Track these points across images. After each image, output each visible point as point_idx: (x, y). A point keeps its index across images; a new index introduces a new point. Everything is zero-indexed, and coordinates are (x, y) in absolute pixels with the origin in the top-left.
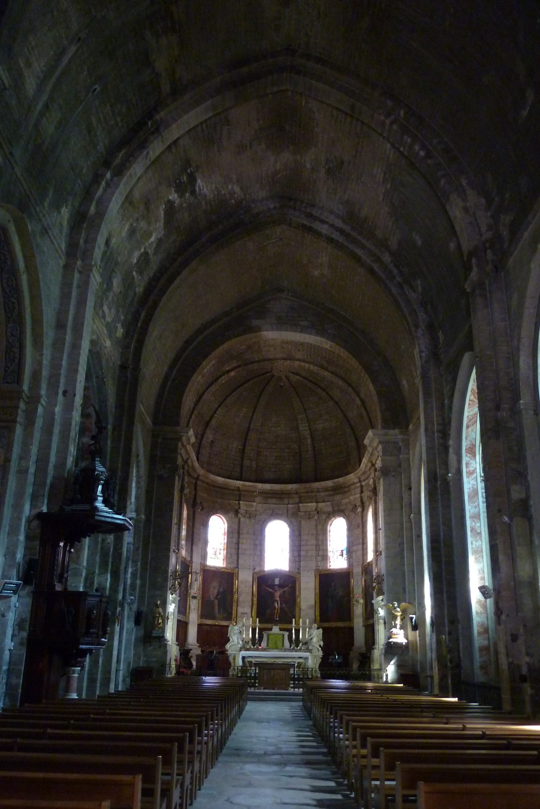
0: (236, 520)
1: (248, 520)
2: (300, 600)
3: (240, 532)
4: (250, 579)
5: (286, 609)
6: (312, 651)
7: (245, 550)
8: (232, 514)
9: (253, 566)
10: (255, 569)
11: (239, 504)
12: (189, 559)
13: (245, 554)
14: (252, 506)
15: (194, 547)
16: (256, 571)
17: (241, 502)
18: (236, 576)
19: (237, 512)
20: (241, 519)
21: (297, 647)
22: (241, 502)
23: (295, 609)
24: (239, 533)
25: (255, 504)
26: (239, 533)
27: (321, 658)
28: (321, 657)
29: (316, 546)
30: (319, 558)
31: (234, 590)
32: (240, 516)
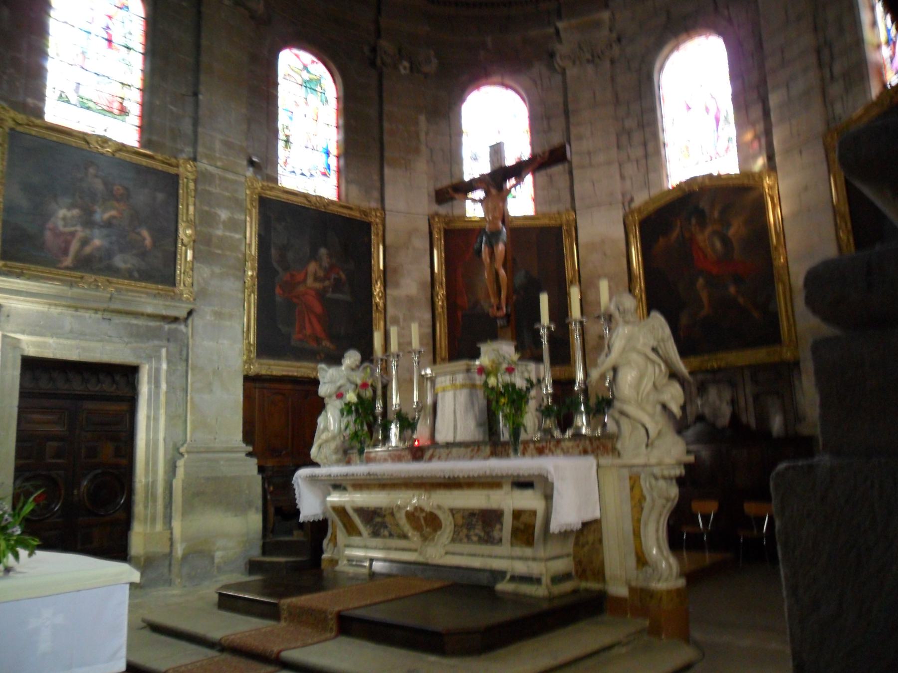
0: (558, 78)
1: (590, 68)
2: (786, 259)
3: (571, 107)
4: (619, 232)
5: (741, 300)
6: (619, 446)
7: (589, 153)
8: (539, 68)
9: (623, 195)
10: (632, 200)
11: (557, 32)
12: (374, 205)
13: (591, 165)
14: (597, 24)
15: (387, 171)
16: (637, 203)
17: (560, 25)
18: (570, 235)
19: (552, 55)
20: (568, 72)
21: (563, 431)
22: (560, 25)
23: (771, 296)
24: (567, 113)
25: (605, 15)
26: (567, 113)
27: (680, 481)
28: (679, 471)
29: (818, 52)
30: (835, 89)
31: (569, 274)
32: (559, 62)
